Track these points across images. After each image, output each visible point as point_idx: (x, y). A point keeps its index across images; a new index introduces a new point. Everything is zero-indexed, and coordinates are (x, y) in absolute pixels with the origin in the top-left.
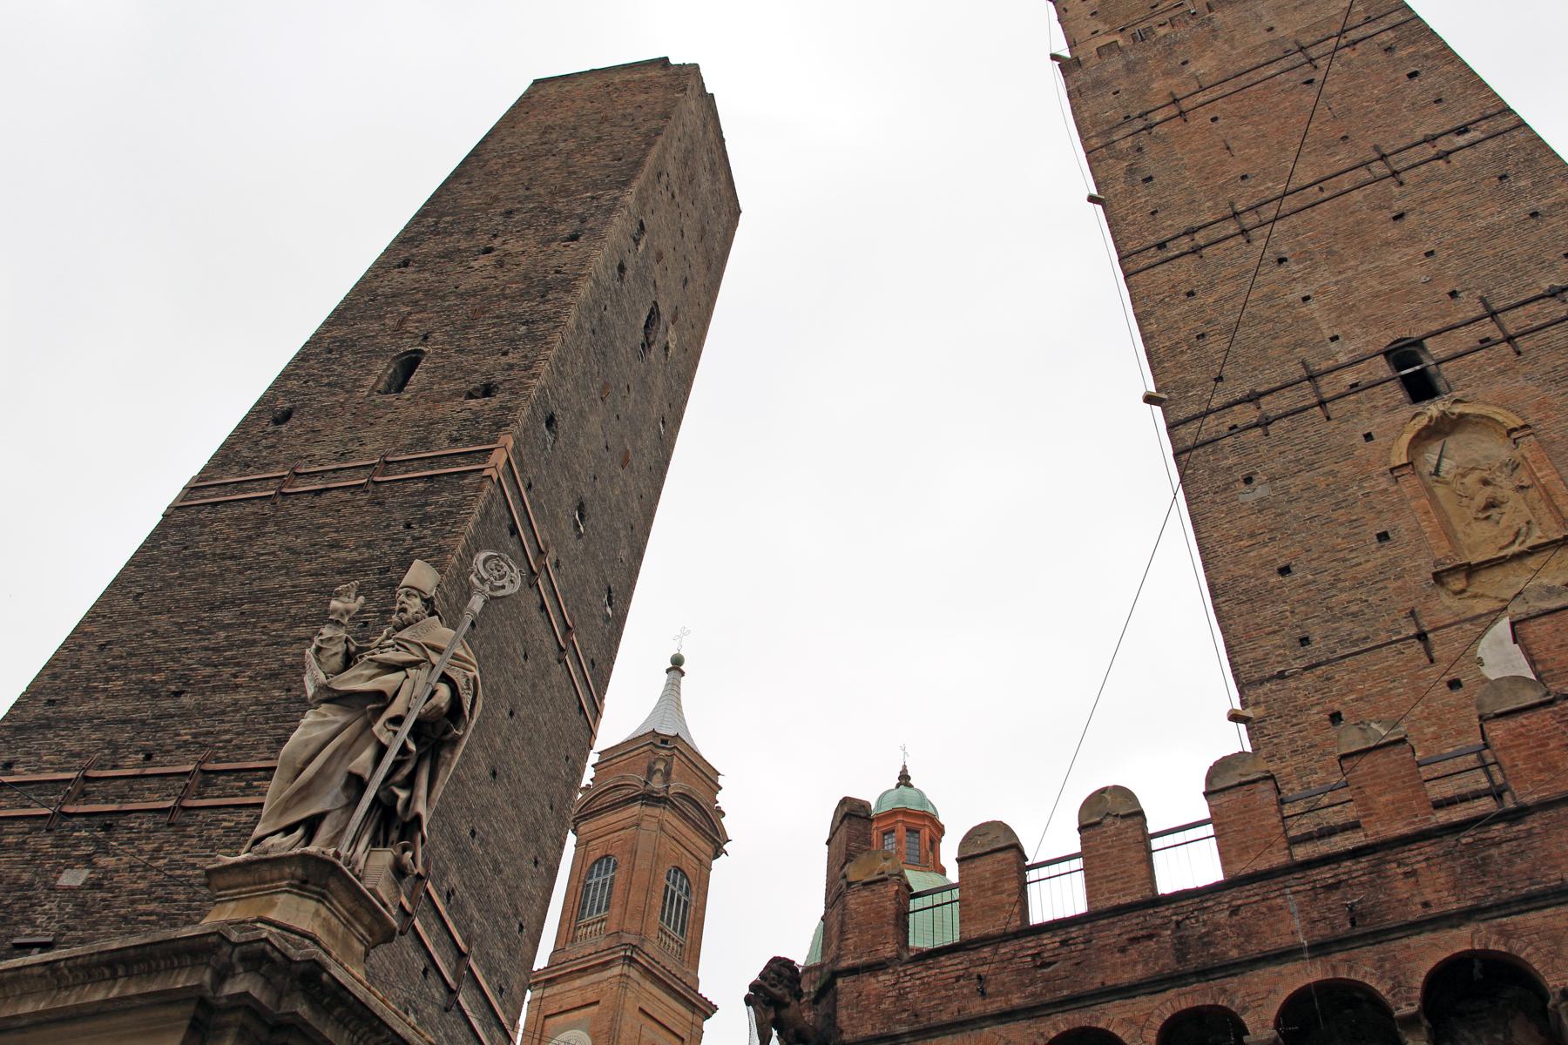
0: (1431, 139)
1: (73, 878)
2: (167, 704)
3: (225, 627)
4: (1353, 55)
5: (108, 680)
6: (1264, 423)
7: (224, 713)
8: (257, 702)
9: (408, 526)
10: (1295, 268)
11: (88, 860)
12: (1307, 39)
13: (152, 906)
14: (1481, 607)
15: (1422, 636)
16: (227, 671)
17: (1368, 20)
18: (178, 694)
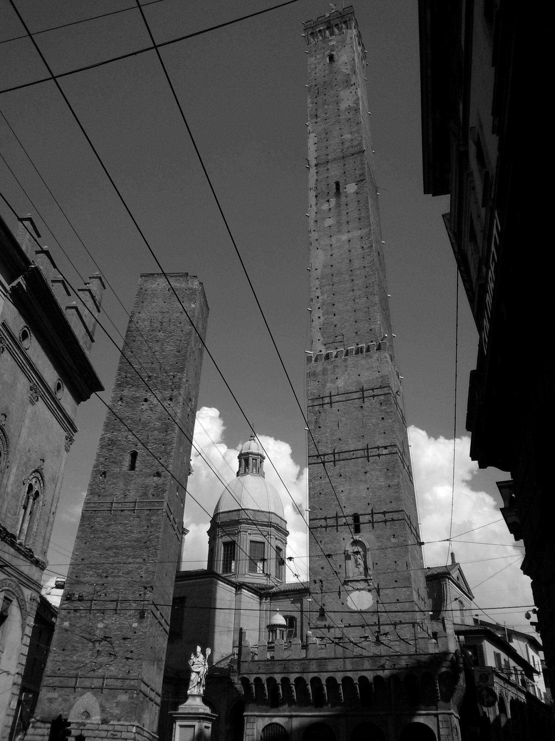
0: (378, 448)
1: (100, 625)
2: (104, 579)
3: (112, 557)
4: (374, 401)
5: (88, 571)
6: (326, 527)
7: (118, 583)
8: (126, 581)
9: (148, 526)
10: (343, 480)
11: (101, 621)
12: (366, 387)
13: (119, 633)
14: (351, 589)
16: (116, 571)
17: (381, 387)
18: (107, 577)
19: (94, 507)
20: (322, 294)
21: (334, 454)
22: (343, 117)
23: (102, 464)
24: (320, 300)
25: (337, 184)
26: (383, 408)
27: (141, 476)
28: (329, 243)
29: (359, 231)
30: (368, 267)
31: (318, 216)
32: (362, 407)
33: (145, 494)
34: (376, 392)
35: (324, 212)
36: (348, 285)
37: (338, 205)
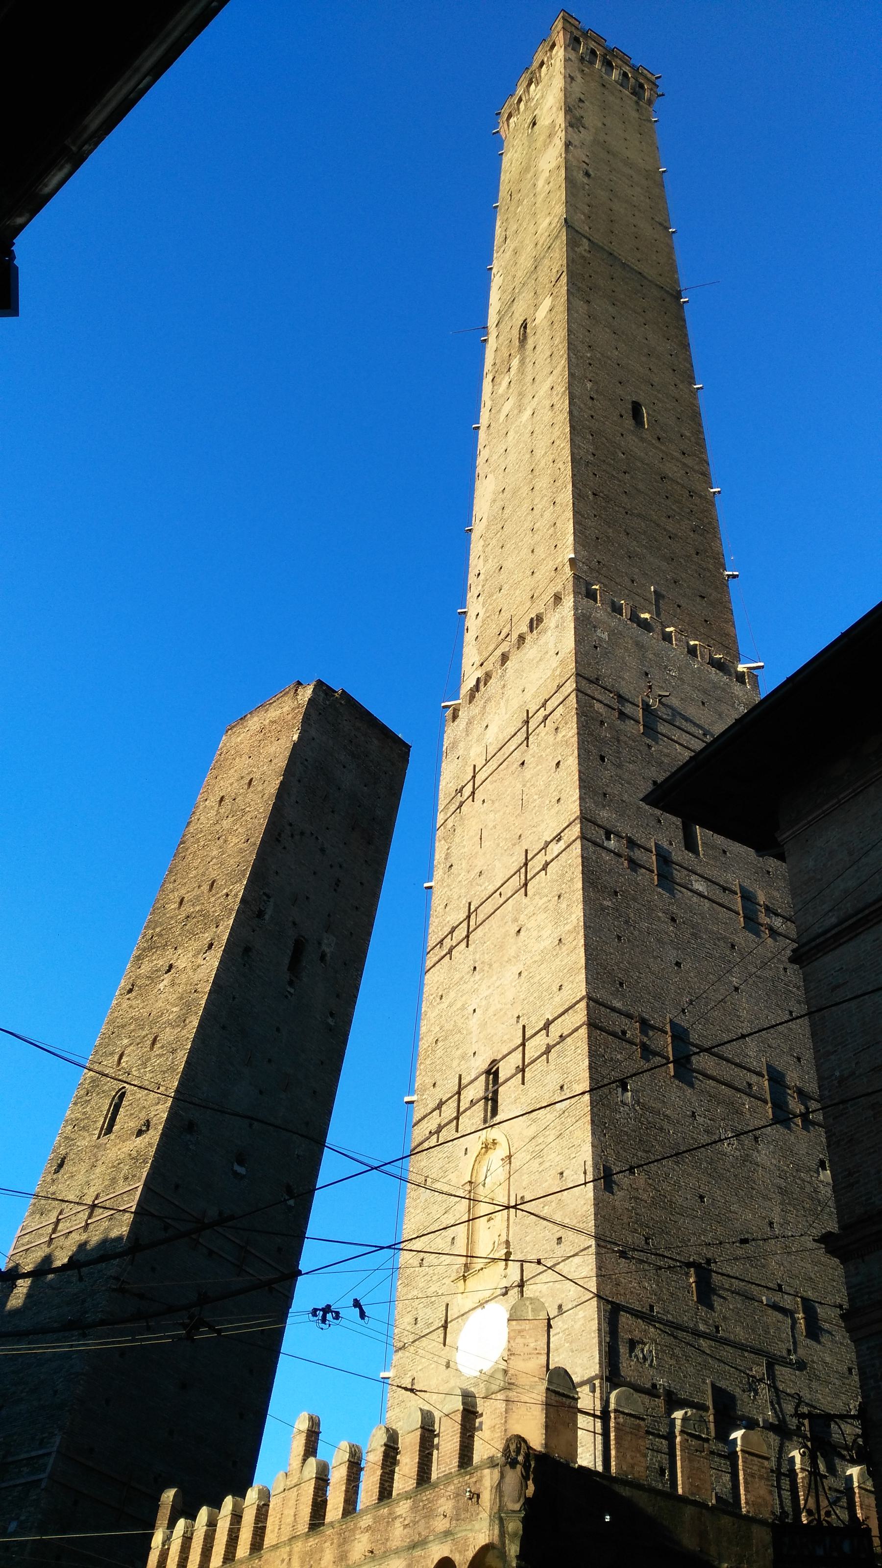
15: (445, 1327)
19: (29, 1242)
20: (486, 561)
21: (469, 917)
22: (540, 199)
23: (66, 1138)
24: (482, 577)
25: (524, 326)
26: (560, 735)
27: (118, 1141)
28: (505, 448)
29: (551, 379)
30: (558, 438)
31: (493, 411)
32: (523, 763)
33: (114, 1180)
34: (550, 706)
35: (502, 395)
36: (526, 505)
37: (522, 362)
